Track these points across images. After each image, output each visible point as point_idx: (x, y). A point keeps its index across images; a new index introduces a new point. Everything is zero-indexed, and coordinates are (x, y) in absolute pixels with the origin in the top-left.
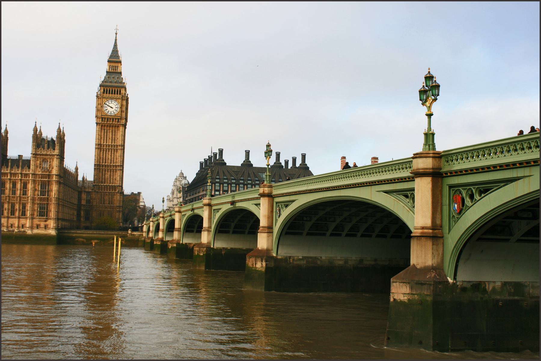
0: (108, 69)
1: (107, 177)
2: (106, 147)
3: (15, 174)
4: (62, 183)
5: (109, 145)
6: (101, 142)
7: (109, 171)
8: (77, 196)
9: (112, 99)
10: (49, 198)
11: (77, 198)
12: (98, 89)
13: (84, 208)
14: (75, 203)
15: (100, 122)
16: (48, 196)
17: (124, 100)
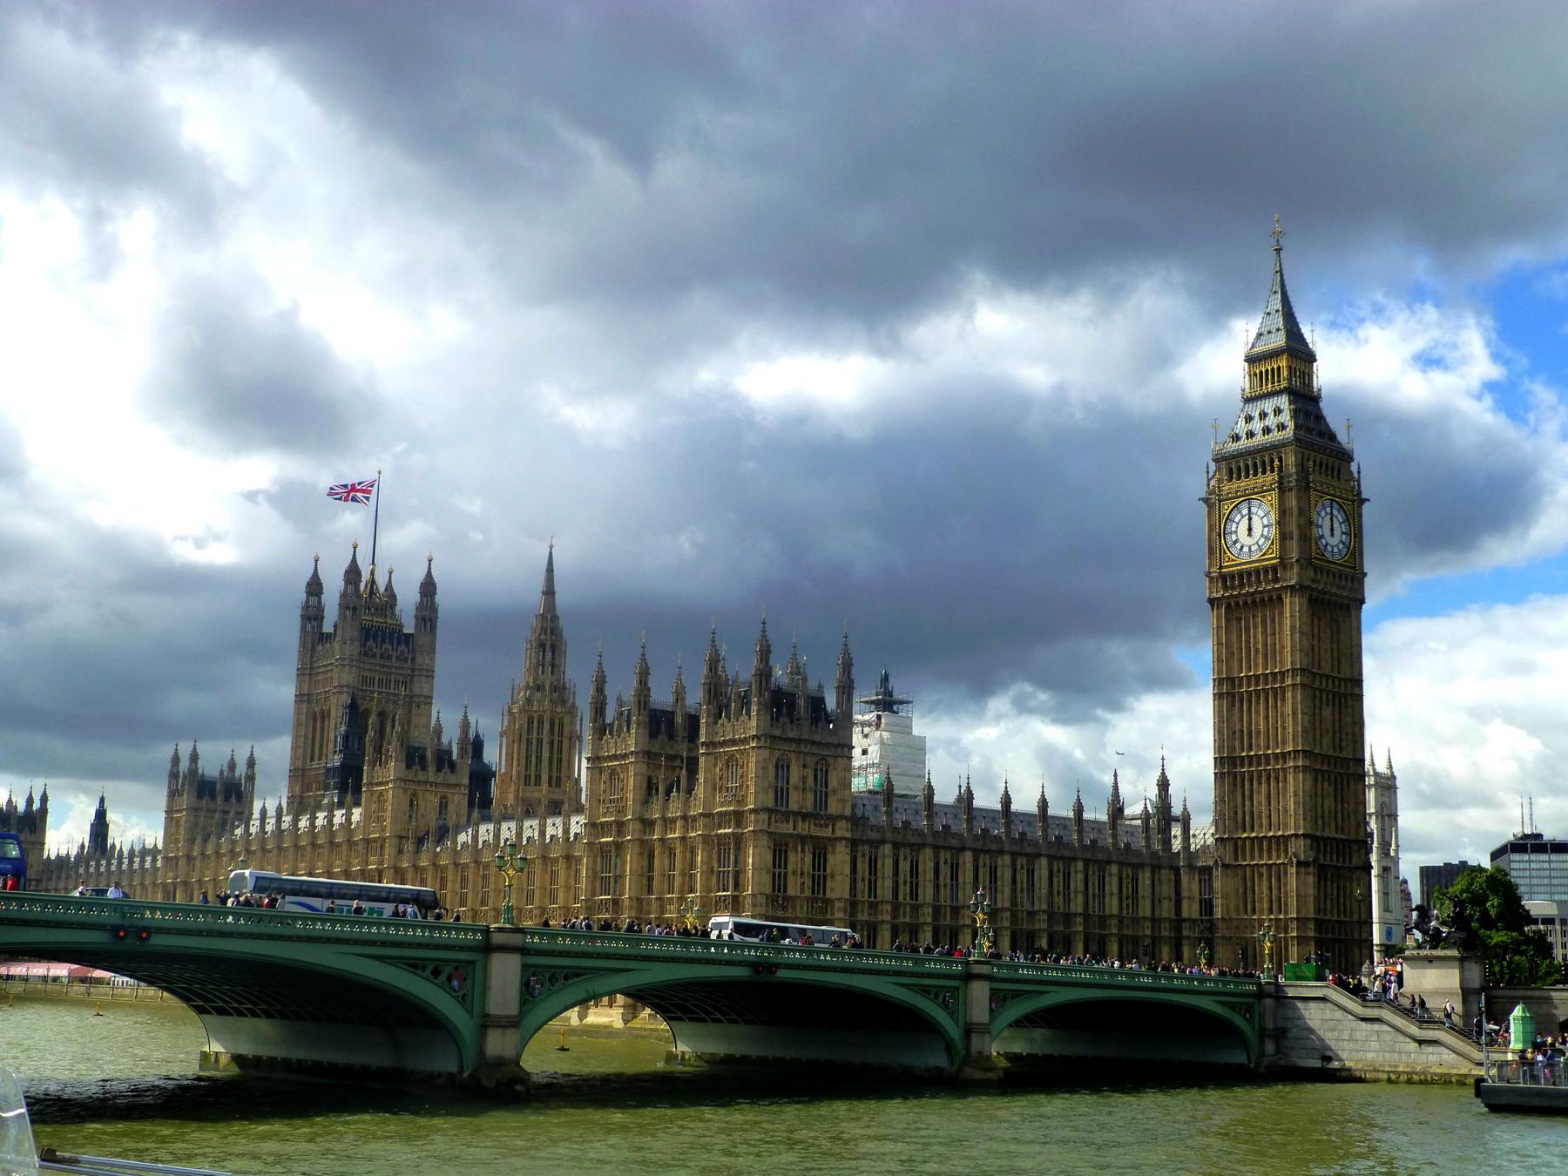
0: (1247, 386)
1: (1260, 804)
2: (1249, 685)
3: (674, 820)
4: (845, 838)
5: (1257, 677)
6: (1229, 669)
7: (1263, 779)
8: (1166, 889)
9: (1248, 496)
10: (741, 899)
11: (1173, 896)
12: (1208, 472)
13: (1194, 933)
14: (1165, 914)
15: (1219, 595)
16: (736, 886)
17: (1291, 490)
